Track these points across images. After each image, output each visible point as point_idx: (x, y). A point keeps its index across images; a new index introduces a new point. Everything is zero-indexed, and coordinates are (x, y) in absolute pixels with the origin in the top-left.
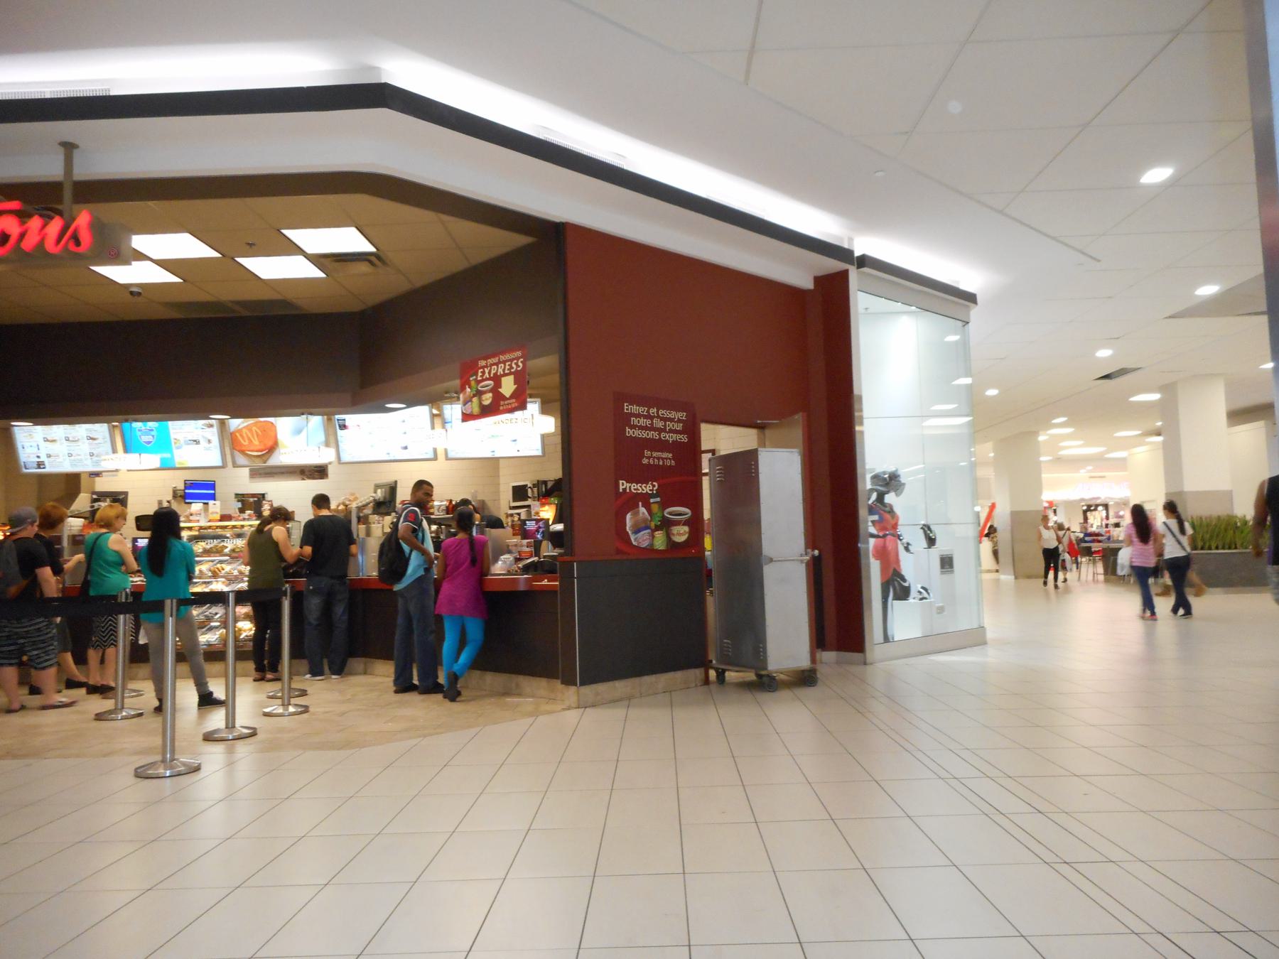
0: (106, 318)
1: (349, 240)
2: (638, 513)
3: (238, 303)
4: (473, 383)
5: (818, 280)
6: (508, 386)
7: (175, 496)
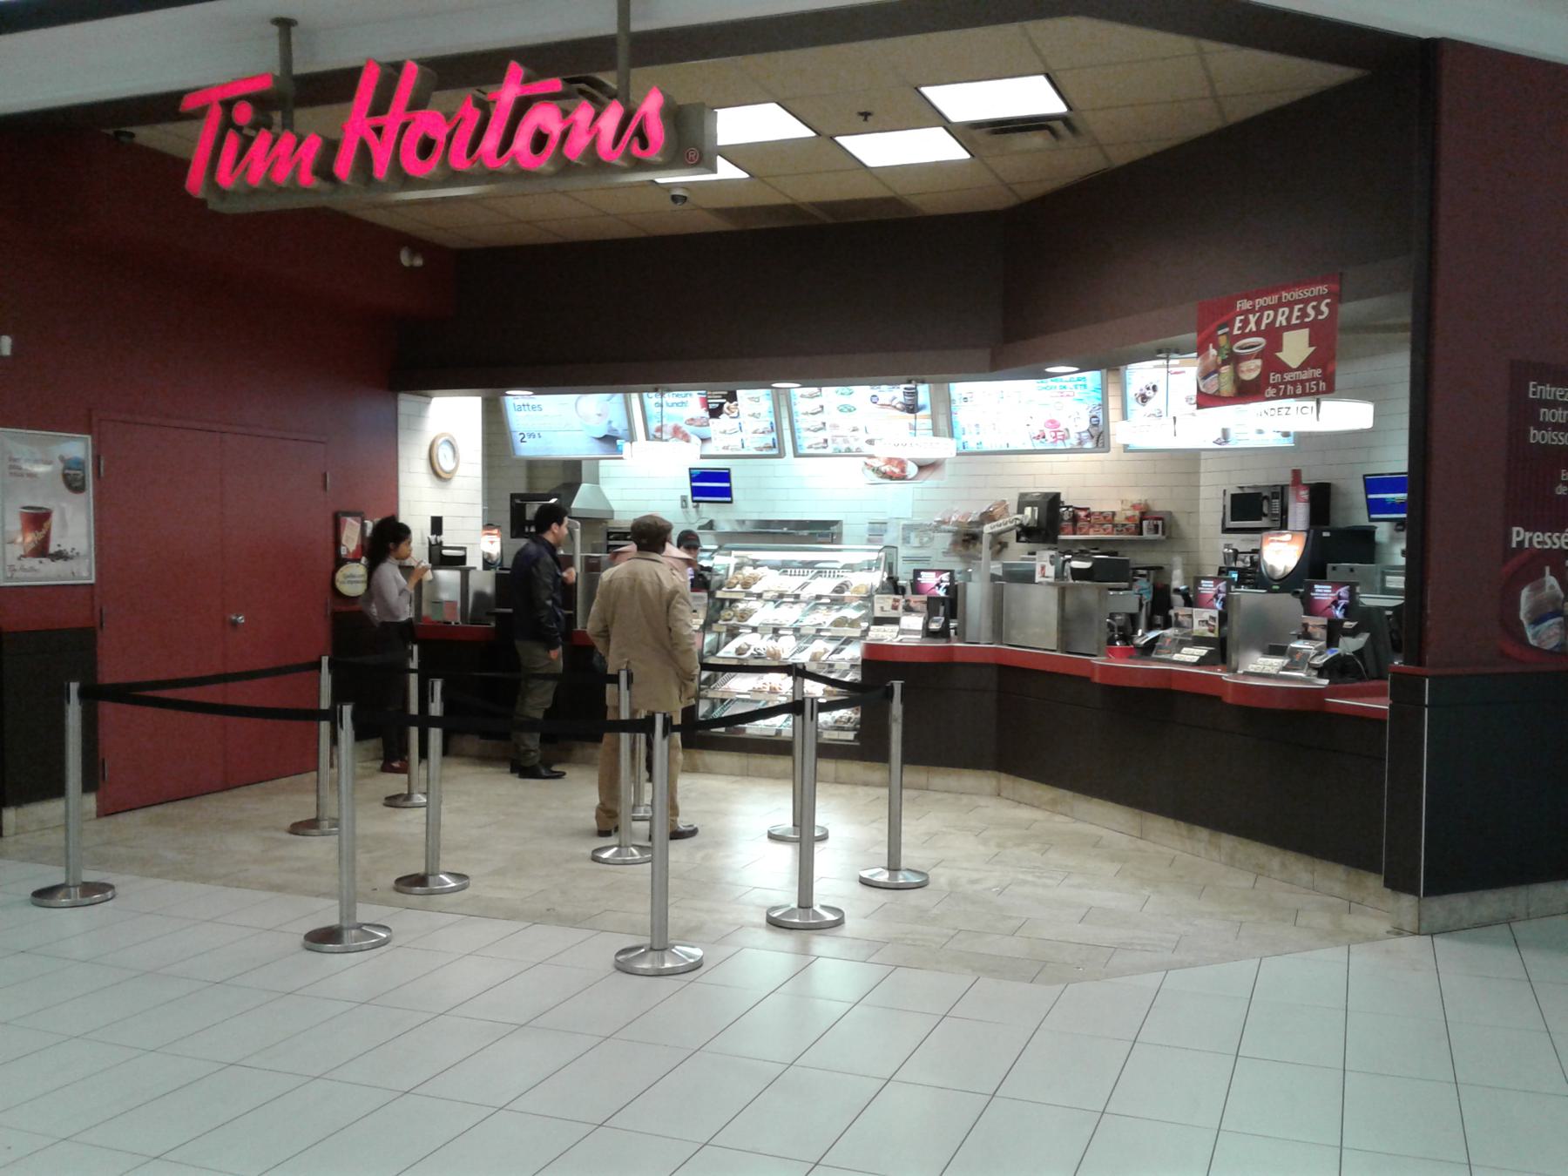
0: (624, 232)
1: (1032, 96)
2: (1541, 587)
3: (813, 204)
4: (1223, 341)
6: (1295, 348)
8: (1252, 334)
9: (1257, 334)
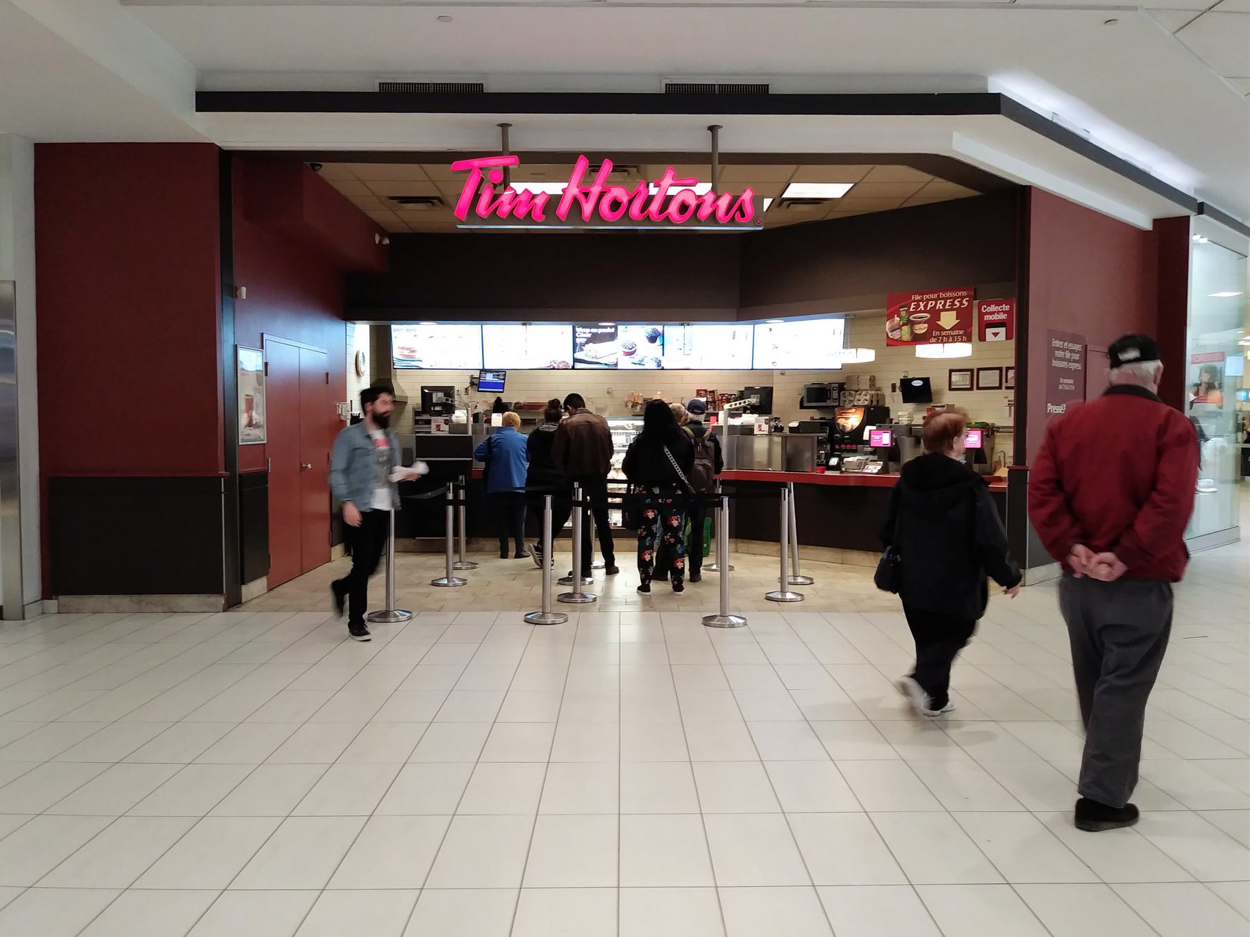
1: (836, 191)
4: (903, 314)
5: (1156, 222)
6: (948, 320)
7: (472, 384)
8: (921, 312)
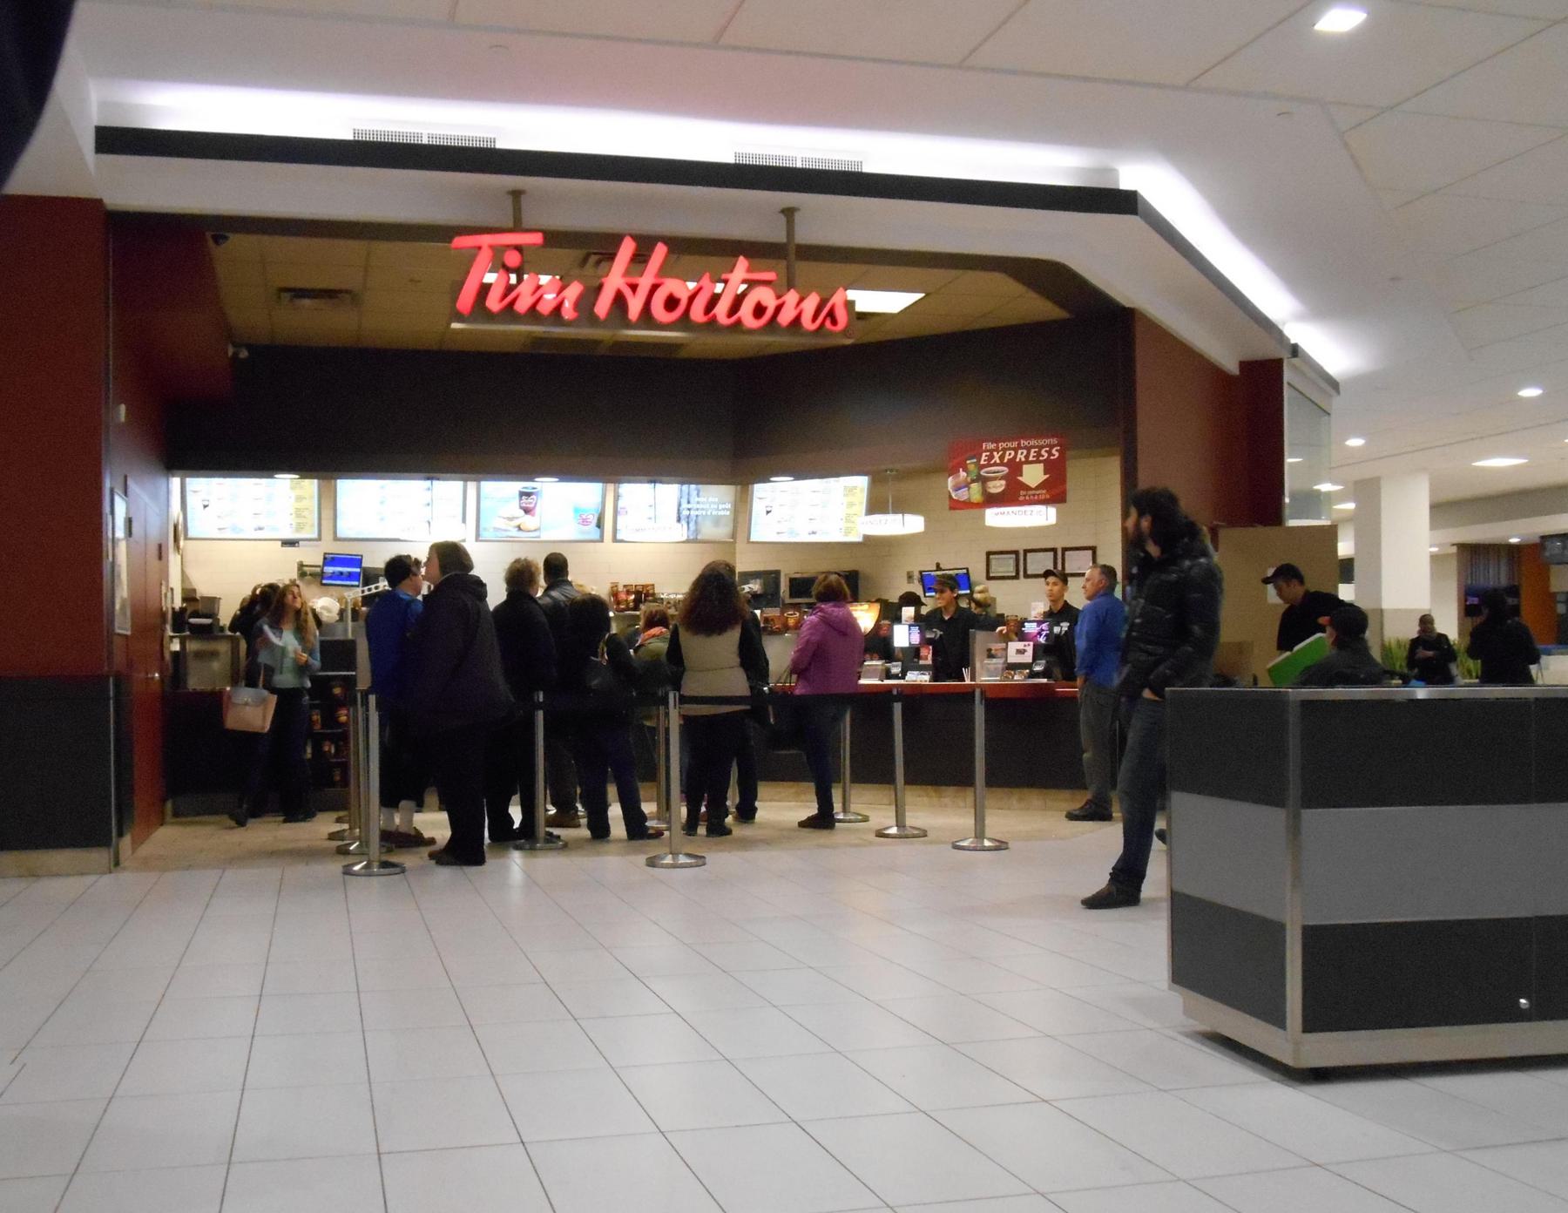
4: (972, 467)
6: (1033, 475)
7: (302, 575)
8: (995, 464)
9: (1002, 464)
